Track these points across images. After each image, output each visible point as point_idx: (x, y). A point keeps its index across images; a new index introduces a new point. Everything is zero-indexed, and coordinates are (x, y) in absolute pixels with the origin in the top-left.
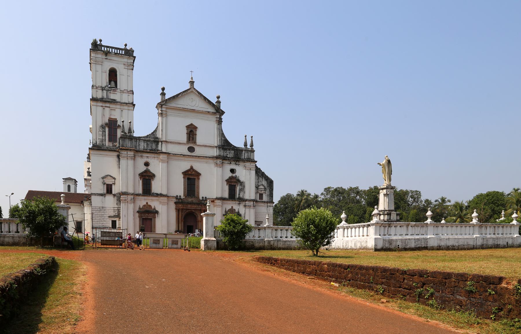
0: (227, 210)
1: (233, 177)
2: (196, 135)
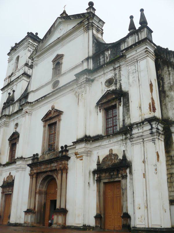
0: (101, 159)
1: (108, 92)
2: (62, 63)
